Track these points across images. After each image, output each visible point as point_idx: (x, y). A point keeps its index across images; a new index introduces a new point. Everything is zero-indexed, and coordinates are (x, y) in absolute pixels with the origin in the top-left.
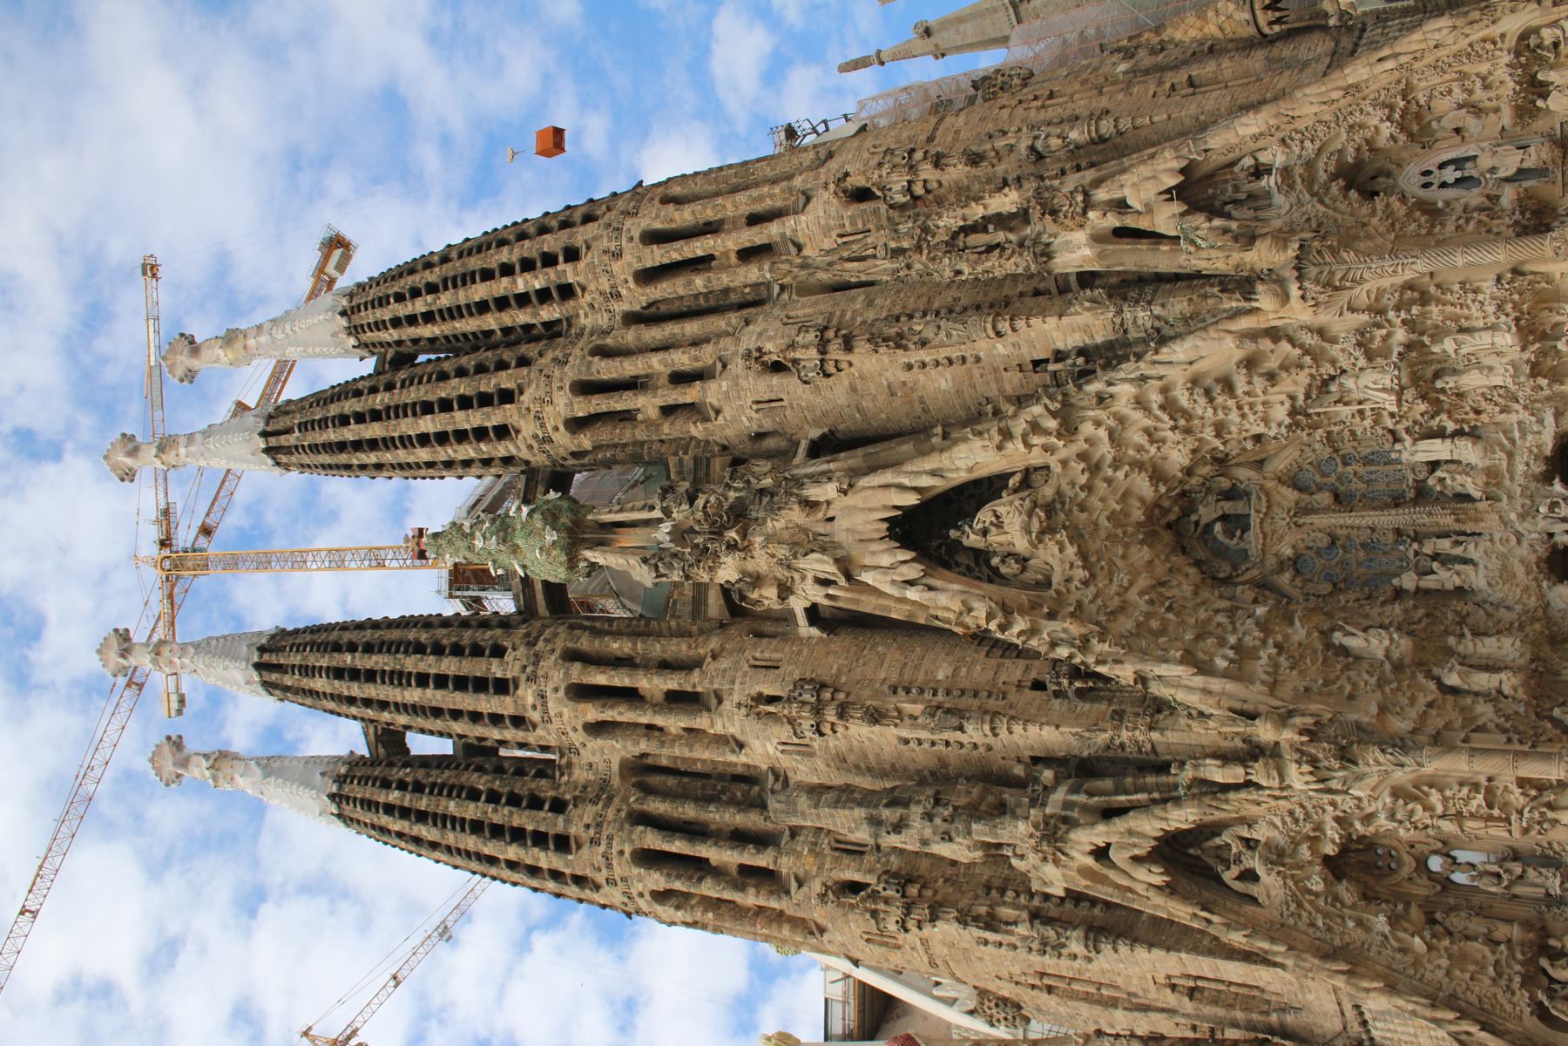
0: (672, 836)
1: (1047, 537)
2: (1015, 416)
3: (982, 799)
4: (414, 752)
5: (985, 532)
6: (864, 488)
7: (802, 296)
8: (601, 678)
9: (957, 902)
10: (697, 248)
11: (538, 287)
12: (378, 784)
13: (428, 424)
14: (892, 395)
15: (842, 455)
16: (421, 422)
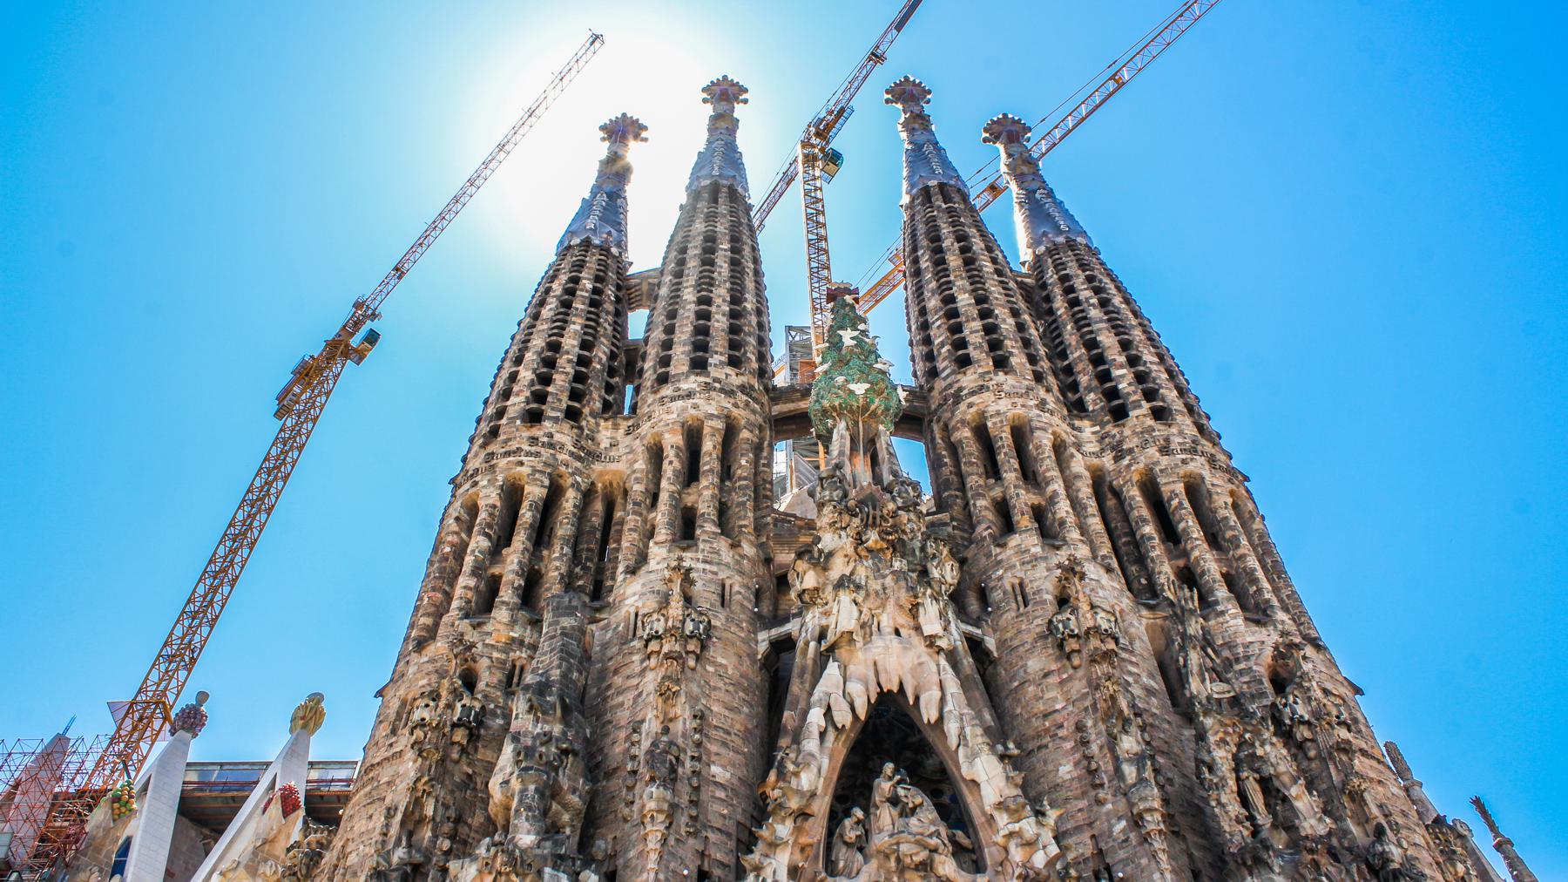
0: (536, 507)
1: (892, 864)
2: (1039, 823)
3: (565, 806)
4: (630, 314)
5: (894, 801)
6: (938, 665)
7: (1147, 630)
8: (709, 445)
9: (442, 783)
10: (1189, 524)
11: (1120, 387)
12: (602, 274)
13: (964, 300)
14: (1046, 716)
15: (971, 660)
16: (967, 295)
